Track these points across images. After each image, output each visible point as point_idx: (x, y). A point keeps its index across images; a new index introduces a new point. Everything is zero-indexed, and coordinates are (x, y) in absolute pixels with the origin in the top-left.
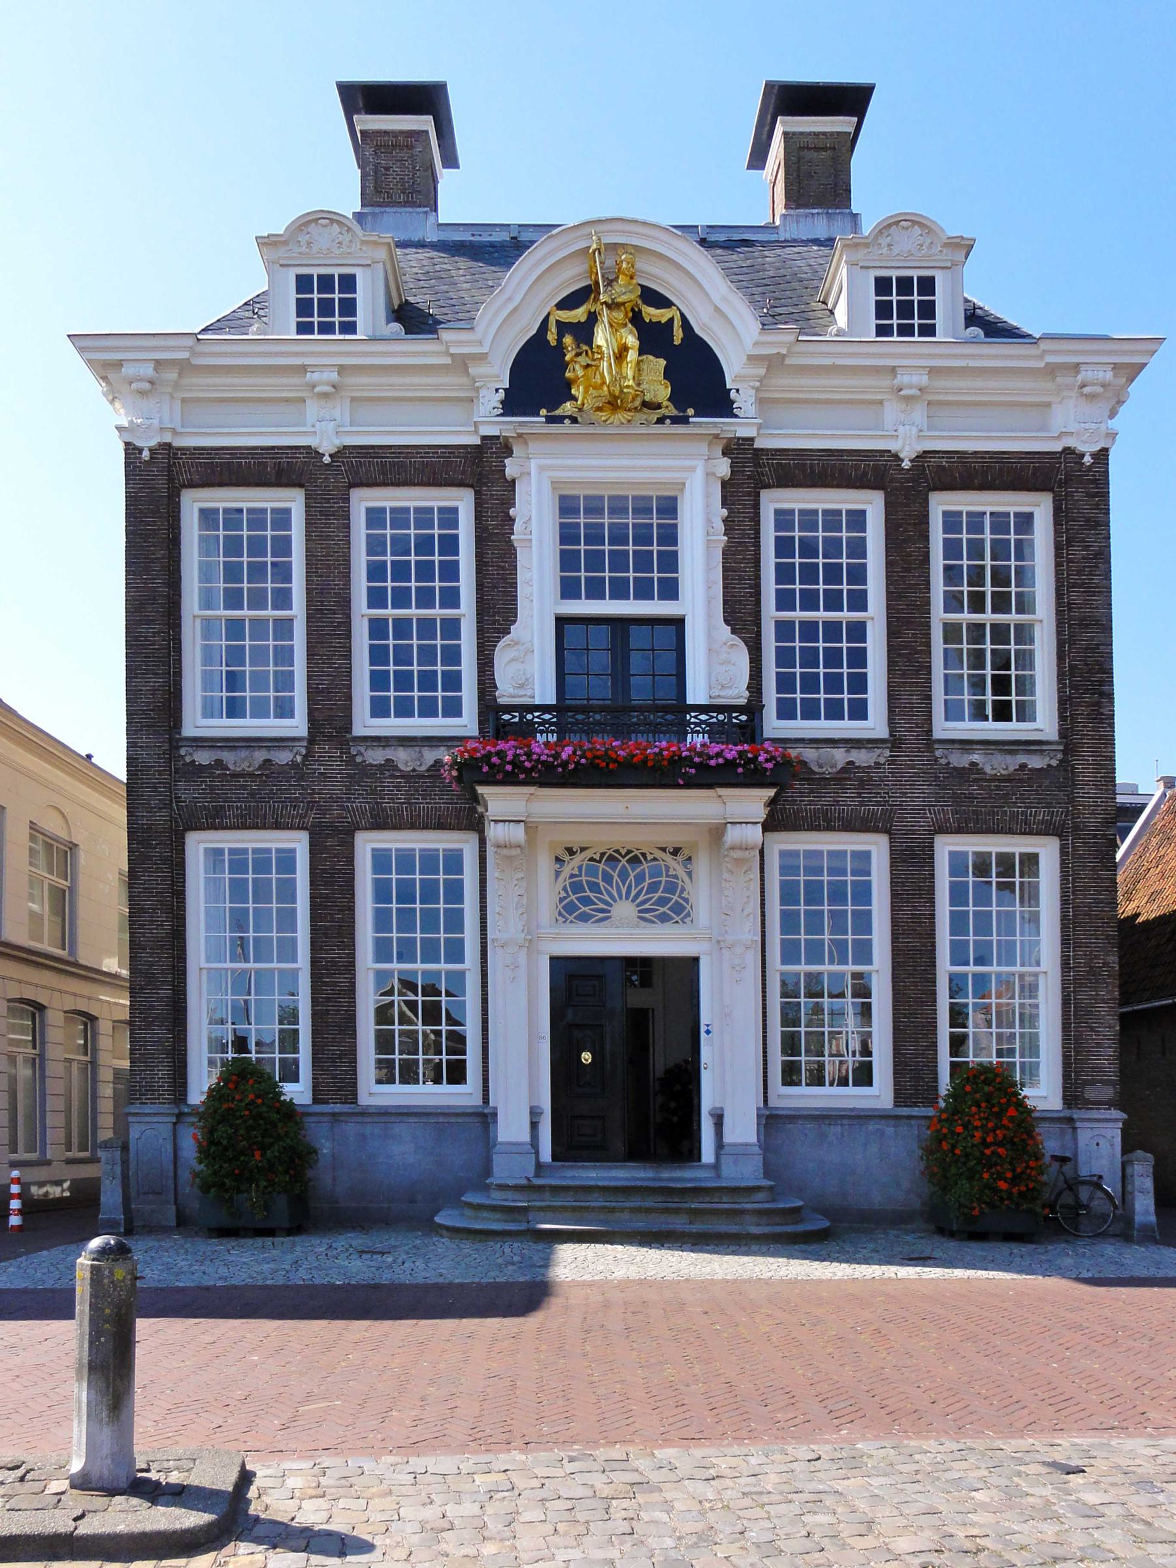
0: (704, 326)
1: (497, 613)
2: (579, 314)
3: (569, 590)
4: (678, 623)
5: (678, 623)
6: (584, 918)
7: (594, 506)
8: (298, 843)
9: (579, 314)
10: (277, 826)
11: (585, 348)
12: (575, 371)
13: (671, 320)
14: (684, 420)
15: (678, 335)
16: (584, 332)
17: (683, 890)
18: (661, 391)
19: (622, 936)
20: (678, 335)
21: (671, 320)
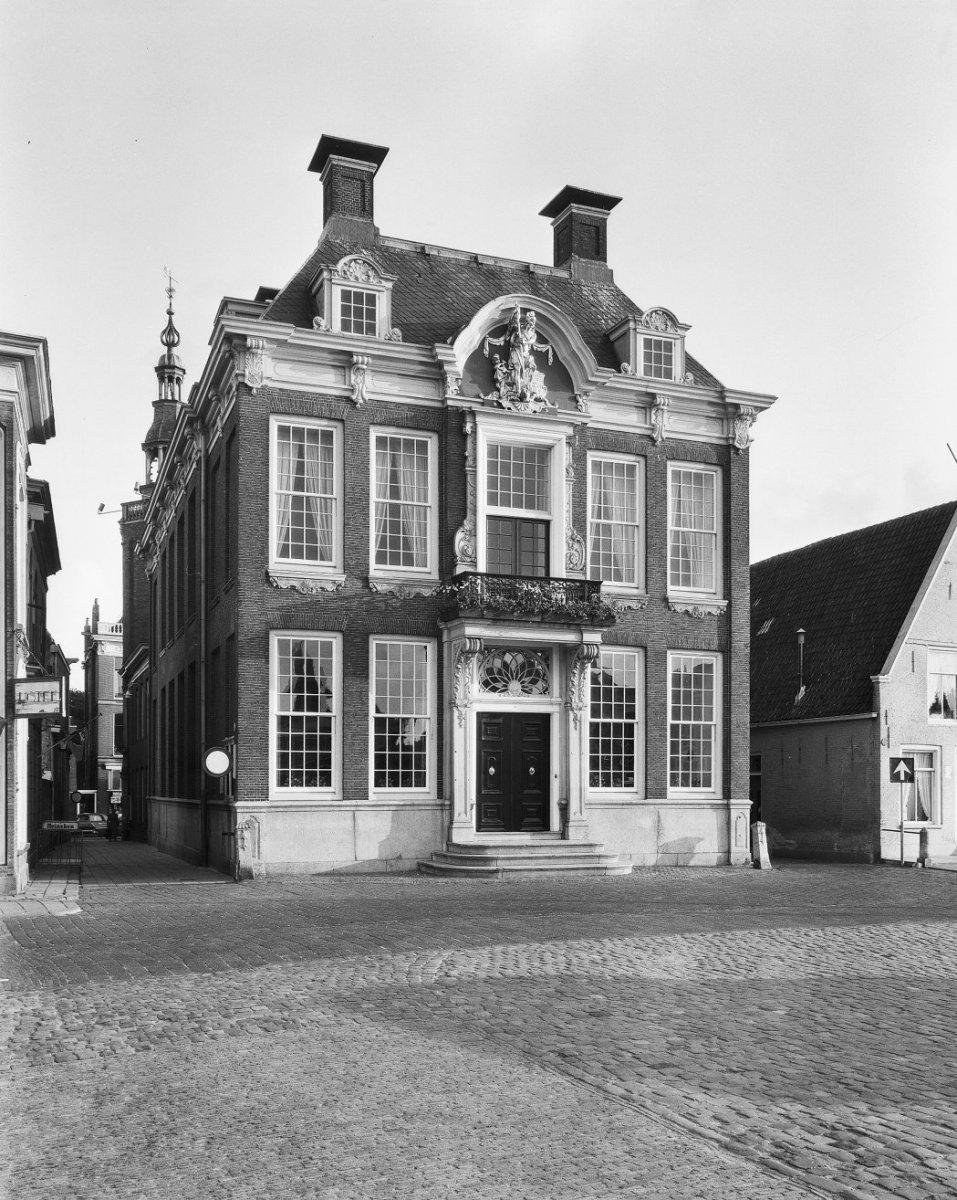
0: (564, 358)
1: (454, 507)
2: (500, 342)
3: (492, 500)
4: (547, 523)
5: (547, 523)
6: (494, 689)
7: (506, 451)
8: (336, 642)
9: (500, 342)
10: (325, 630)
11: (504, 362)
12: (499, 376)
13: (548, 351)
14: (554, 412)
15: (551, 360)
16: (505, 352)
17: (544, 675)
18: (542, 393)
19: (513, 701)
20: (551, 360)
21: (548, 351)
